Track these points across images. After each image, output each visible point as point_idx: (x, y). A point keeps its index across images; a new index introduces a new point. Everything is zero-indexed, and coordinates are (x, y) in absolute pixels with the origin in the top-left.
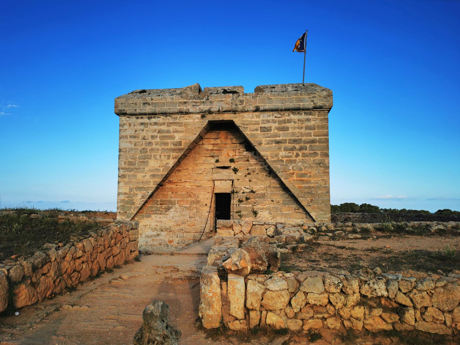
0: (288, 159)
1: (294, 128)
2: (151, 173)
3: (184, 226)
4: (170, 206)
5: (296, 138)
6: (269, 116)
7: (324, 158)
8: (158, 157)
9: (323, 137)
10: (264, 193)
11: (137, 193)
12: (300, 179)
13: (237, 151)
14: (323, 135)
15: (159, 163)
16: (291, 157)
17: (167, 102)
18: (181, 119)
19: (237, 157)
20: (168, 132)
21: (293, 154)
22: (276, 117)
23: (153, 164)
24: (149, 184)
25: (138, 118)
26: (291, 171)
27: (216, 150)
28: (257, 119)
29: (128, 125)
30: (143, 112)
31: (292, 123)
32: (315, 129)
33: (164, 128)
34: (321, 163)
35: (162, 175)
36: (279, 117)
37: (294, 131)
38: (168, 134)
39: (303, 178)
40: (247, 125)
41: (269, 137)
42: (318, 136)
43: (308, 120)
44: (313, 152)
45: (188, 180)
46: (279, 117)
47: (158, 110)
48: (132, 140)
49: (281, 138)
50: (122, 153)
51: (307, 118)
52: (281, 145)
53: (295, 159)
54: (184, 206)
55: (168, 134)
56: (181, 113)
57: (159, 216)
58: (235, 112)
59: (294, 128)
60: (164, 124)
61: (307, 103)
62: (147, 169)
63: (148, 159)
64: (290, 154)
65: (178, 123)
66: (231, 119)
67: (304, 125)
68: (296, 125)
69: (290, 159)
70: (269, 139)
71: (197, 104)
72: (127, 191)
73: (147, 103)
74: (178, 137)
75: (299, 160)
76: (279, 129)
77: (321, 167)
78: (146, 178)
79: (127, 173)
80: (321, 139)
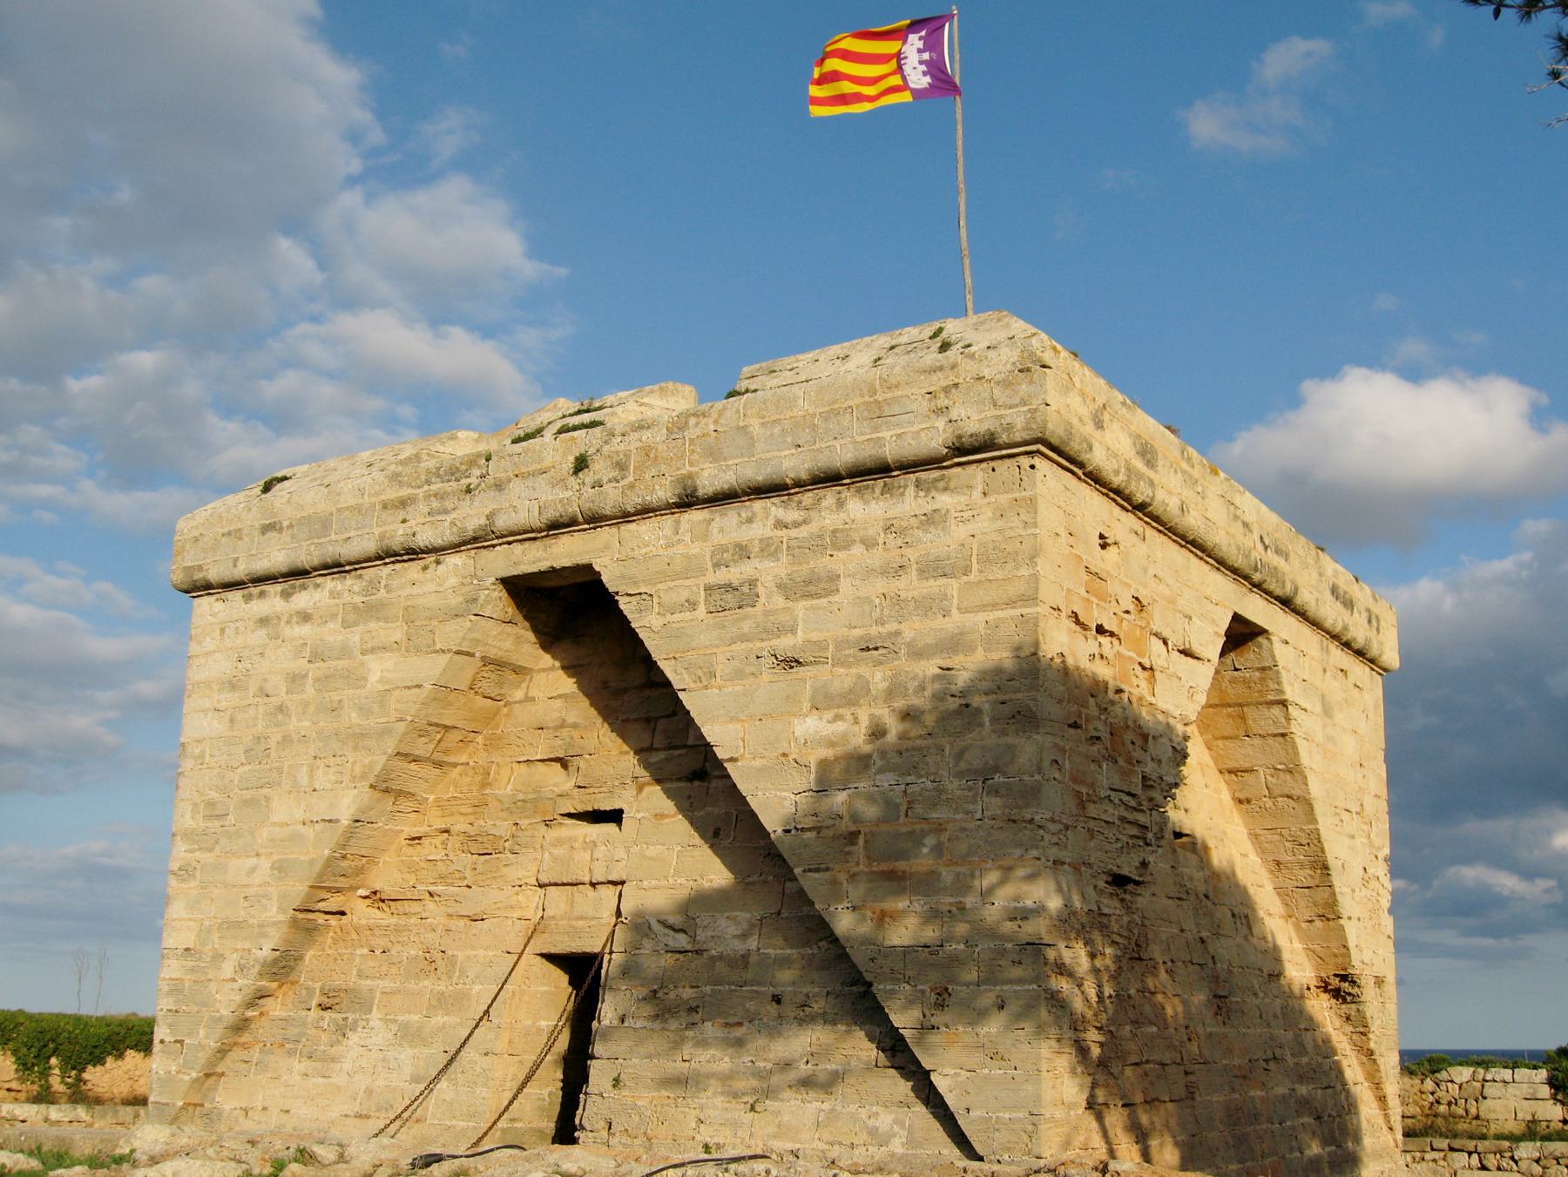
2: (275, 857)
4: (351, 1017)
5: (874, 631)
6: (750, 520)
7: (1010, 740)
12: (884, 867)
14: (1011, 604)
17: (339, 510)
18: (395, 583)
20: (344, 651)
21: (856, 721)
22: (781, 524)
23: (285, 810)
25: (248, 598)
28: (695, 549)
29: (217, 634)
30: (262, 565)
31: (858, 550)
33: (333, 633)
34: (996, 769)
35: (312, 862)
36: (797, 525)
41: (744, 638)
42: (982, 608)
43: (931, 520)
45: (439, 888)
46: (797, 525)
47: (307, 555)
48: (227, 699)
51: (928, 508)
54: (400, 1018)
56: (387, 555)
58: (595, 520)
59: (870, 572)
61: (915, 428)
62: (264, 834)
63: (270, 785)
64: (840, 727)
65: (383, 605)
66: (582, 560)
67: (912, 554)
68: (876, 558)
70: (744, 646)
71: (449, 505)
74: (378, 670)
76: (789, 589)
77: (995, 792)
78: (257, 878)
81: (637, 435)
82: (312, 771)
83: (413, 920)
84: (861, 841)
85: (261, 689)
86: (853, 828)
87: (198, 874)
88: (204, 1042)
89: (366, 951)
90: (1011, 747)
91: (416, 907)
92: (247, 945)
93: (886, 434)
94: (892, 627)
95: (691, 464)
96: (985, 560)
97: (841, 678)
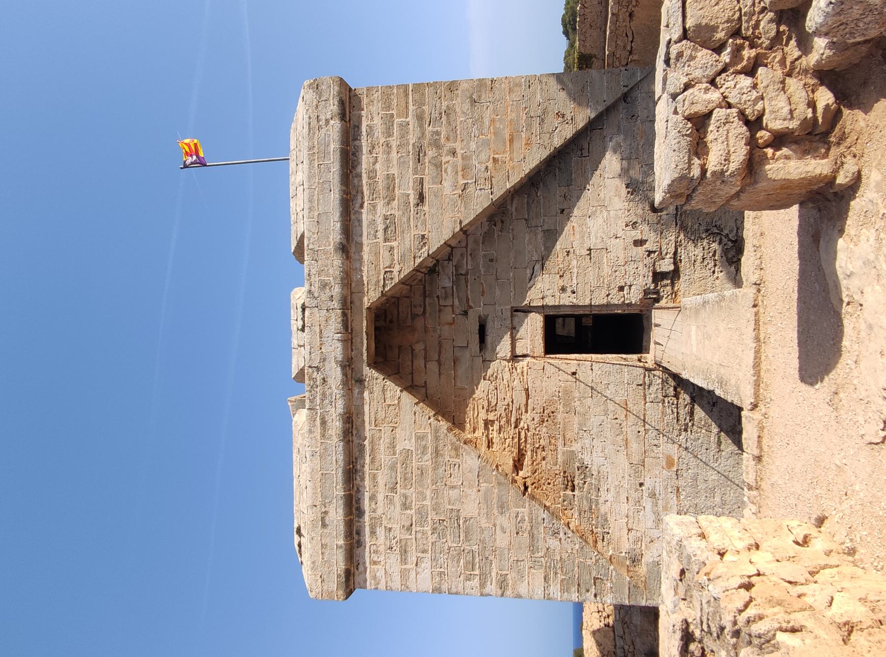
0: (460, 173)
1: (388, 160)
2: (496, 511)
3: (629, 430)
4: (577, 464)
8: (454, 493)
9: (410, 97)
10: (544, 231)
11: (544, 550)
13: (442, 303)
14: (407, 95)
15: (469, 491)
16: (455, 166)
19: (456, 302)
20: (393, 468)
23: (470, 508)
24: (523, 520)
26: (490, 164)
27: (440, 353)
31: (378, 166)
32: (392, 115)
34: (471, 97)
36: (363, 198)
37: (395, 162)
38: (399, 465)
39: (507, 137)
40: (379, 274)
42: (407, 107)
44: (444, 117)
45: (513, 420)
47: (339, 491)
49: (411, 192)
50: (445, 587)
52: (426, 190)
53: (459, 156)
55: (399, 465)
57: (603, 493)
60: (374, 477)
62: (484, 523)
64: (449, 170)
68: (381, 157)
69: (460, 169)
72: (539, 574)
73: (323, 519)
74: (405, 443)
75: (462, 149)
77: (480, 97)
78: (506, 525)
79: (494, 574)
80: (414, 101)
81: (313, 277)
82: (453, 487)
83: (529, 434)
84: (496, 156)
85: (408, 529)
86: (491, 160)
87: (504, 573)
88: (594, 560)
89: (544, 462)
90: (463, 91)
91: (523, 434)
92: (542, 529)
93: (332, 146)
94: (411, 147)
95: (329, 245)
96: (389, 107)
97: (429, 172)
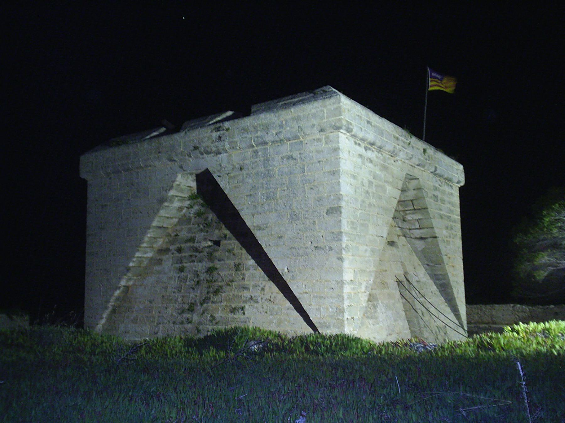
26: (449, 256)
